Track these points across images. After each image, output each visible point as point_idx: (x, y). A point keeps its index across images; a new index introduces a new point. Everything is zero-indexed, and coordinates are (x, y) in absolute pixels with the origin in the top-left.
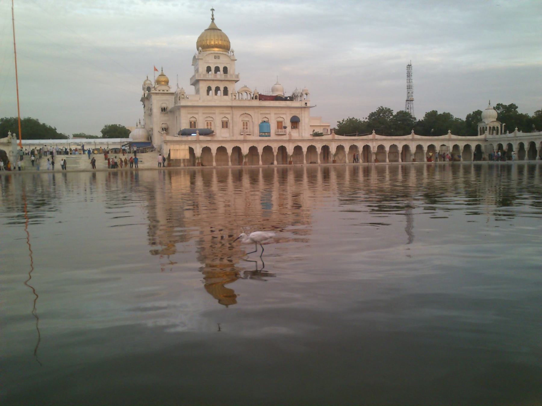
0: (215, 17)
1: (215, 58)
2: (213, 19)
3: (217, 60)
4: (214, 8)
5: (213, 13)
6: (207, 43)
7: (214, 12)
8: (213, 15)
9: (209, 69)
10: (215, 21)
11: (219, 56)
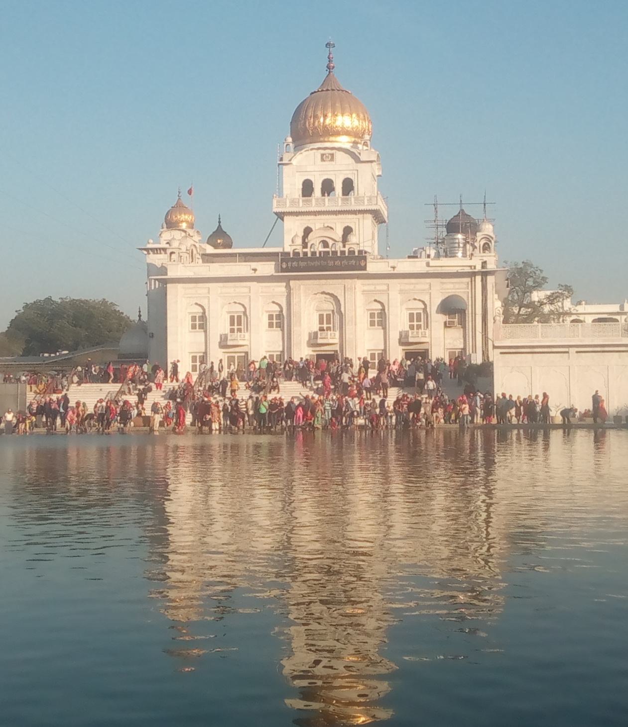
1: (323, 160)
3: (328, 165)
11: (332, 155)
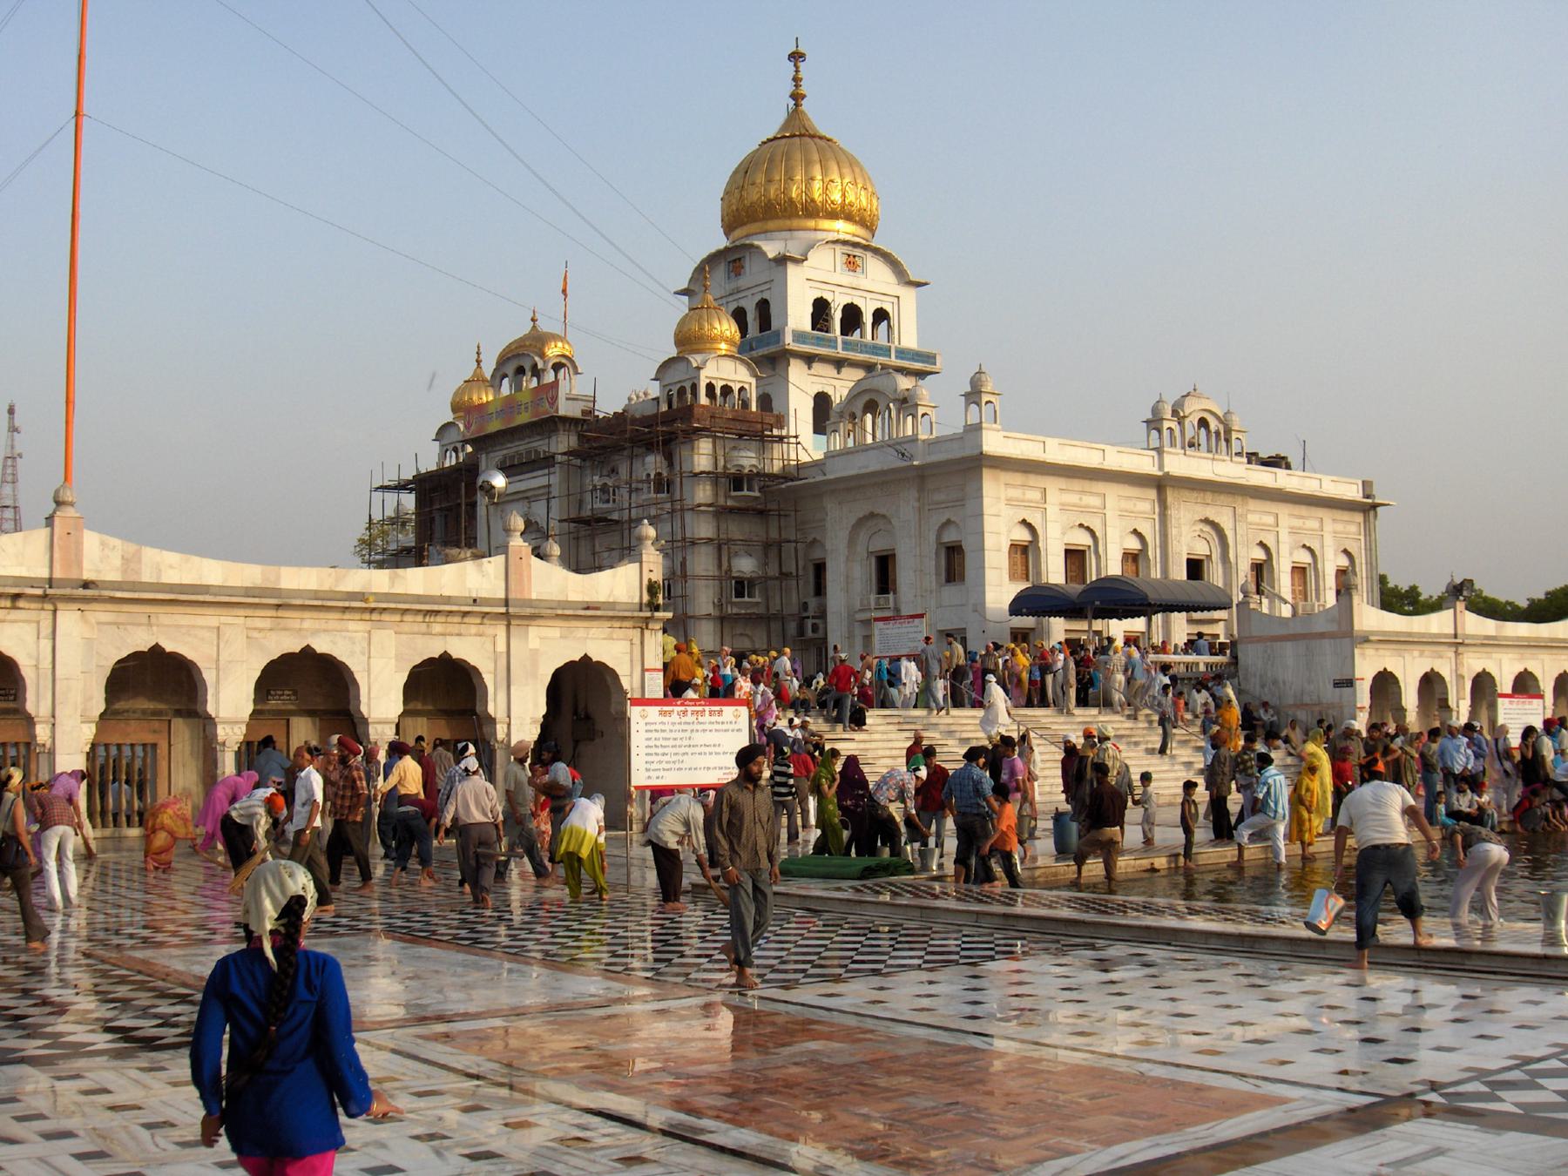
0: (804, 89)
2: (797, 97)
4: (801, 49)
5: (797, 71)
6: (786, 191)
7: (802, 65)
8: (797, 80)
9: (821, 308)
10: (806, 105)
